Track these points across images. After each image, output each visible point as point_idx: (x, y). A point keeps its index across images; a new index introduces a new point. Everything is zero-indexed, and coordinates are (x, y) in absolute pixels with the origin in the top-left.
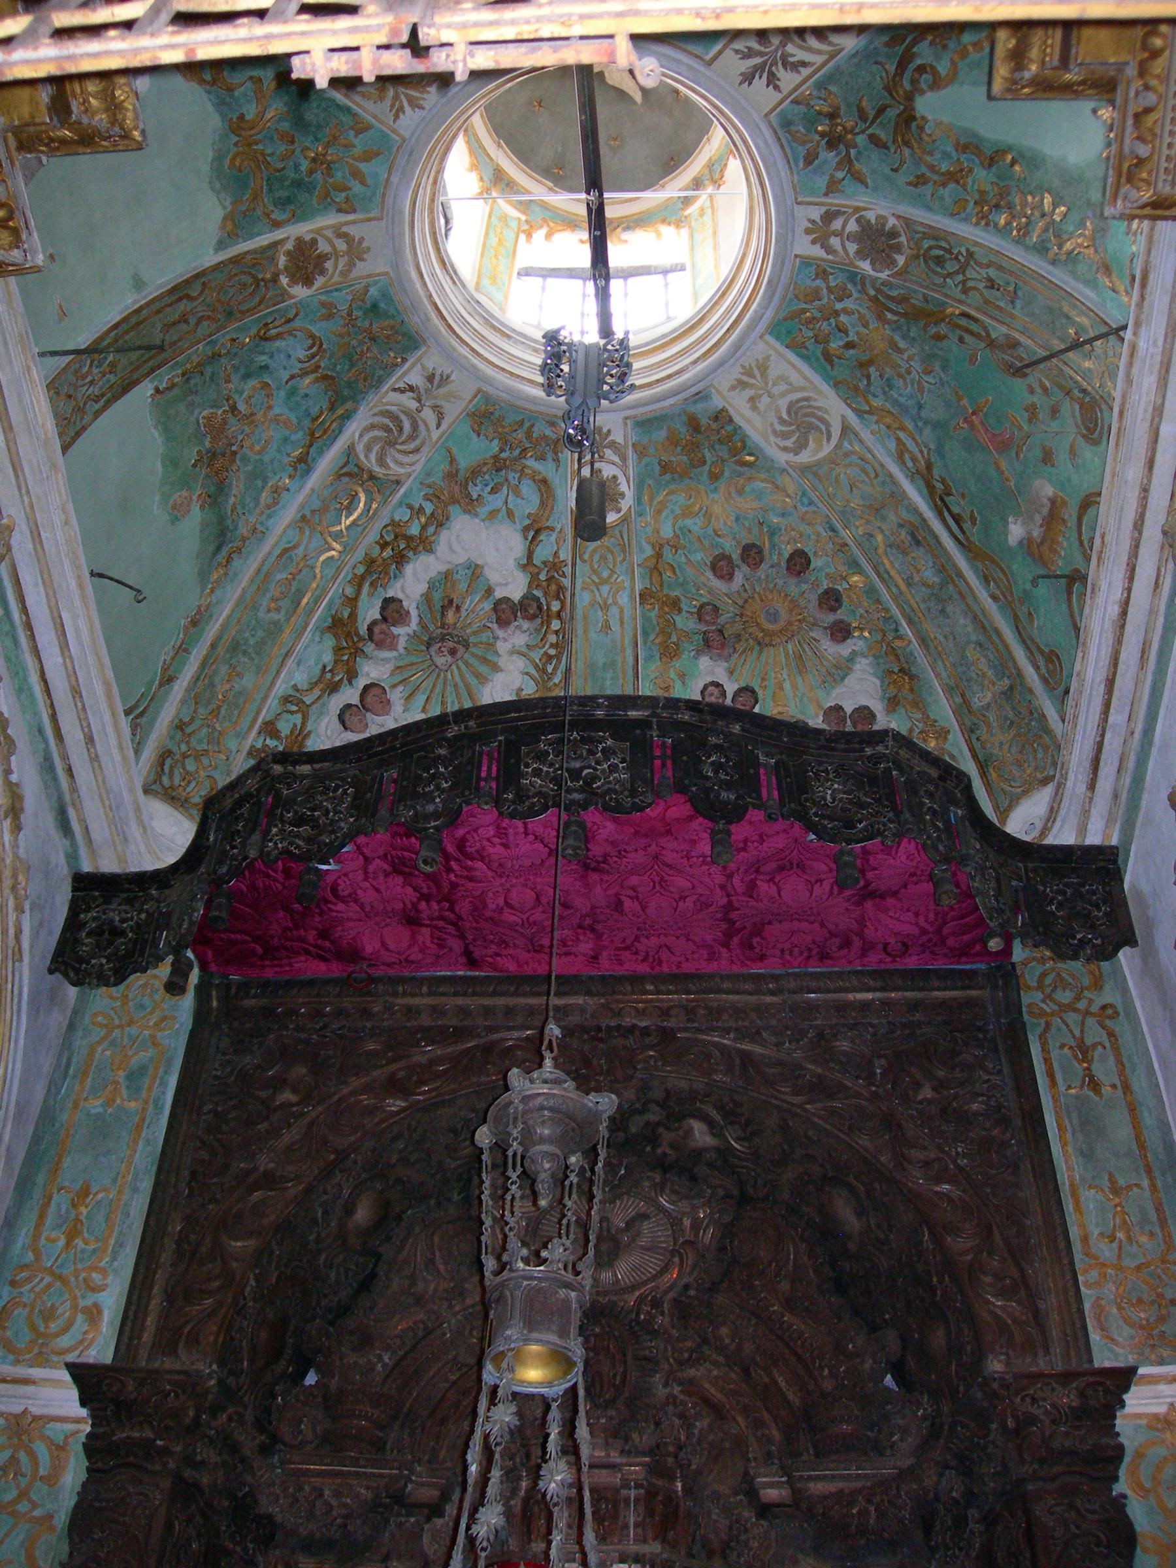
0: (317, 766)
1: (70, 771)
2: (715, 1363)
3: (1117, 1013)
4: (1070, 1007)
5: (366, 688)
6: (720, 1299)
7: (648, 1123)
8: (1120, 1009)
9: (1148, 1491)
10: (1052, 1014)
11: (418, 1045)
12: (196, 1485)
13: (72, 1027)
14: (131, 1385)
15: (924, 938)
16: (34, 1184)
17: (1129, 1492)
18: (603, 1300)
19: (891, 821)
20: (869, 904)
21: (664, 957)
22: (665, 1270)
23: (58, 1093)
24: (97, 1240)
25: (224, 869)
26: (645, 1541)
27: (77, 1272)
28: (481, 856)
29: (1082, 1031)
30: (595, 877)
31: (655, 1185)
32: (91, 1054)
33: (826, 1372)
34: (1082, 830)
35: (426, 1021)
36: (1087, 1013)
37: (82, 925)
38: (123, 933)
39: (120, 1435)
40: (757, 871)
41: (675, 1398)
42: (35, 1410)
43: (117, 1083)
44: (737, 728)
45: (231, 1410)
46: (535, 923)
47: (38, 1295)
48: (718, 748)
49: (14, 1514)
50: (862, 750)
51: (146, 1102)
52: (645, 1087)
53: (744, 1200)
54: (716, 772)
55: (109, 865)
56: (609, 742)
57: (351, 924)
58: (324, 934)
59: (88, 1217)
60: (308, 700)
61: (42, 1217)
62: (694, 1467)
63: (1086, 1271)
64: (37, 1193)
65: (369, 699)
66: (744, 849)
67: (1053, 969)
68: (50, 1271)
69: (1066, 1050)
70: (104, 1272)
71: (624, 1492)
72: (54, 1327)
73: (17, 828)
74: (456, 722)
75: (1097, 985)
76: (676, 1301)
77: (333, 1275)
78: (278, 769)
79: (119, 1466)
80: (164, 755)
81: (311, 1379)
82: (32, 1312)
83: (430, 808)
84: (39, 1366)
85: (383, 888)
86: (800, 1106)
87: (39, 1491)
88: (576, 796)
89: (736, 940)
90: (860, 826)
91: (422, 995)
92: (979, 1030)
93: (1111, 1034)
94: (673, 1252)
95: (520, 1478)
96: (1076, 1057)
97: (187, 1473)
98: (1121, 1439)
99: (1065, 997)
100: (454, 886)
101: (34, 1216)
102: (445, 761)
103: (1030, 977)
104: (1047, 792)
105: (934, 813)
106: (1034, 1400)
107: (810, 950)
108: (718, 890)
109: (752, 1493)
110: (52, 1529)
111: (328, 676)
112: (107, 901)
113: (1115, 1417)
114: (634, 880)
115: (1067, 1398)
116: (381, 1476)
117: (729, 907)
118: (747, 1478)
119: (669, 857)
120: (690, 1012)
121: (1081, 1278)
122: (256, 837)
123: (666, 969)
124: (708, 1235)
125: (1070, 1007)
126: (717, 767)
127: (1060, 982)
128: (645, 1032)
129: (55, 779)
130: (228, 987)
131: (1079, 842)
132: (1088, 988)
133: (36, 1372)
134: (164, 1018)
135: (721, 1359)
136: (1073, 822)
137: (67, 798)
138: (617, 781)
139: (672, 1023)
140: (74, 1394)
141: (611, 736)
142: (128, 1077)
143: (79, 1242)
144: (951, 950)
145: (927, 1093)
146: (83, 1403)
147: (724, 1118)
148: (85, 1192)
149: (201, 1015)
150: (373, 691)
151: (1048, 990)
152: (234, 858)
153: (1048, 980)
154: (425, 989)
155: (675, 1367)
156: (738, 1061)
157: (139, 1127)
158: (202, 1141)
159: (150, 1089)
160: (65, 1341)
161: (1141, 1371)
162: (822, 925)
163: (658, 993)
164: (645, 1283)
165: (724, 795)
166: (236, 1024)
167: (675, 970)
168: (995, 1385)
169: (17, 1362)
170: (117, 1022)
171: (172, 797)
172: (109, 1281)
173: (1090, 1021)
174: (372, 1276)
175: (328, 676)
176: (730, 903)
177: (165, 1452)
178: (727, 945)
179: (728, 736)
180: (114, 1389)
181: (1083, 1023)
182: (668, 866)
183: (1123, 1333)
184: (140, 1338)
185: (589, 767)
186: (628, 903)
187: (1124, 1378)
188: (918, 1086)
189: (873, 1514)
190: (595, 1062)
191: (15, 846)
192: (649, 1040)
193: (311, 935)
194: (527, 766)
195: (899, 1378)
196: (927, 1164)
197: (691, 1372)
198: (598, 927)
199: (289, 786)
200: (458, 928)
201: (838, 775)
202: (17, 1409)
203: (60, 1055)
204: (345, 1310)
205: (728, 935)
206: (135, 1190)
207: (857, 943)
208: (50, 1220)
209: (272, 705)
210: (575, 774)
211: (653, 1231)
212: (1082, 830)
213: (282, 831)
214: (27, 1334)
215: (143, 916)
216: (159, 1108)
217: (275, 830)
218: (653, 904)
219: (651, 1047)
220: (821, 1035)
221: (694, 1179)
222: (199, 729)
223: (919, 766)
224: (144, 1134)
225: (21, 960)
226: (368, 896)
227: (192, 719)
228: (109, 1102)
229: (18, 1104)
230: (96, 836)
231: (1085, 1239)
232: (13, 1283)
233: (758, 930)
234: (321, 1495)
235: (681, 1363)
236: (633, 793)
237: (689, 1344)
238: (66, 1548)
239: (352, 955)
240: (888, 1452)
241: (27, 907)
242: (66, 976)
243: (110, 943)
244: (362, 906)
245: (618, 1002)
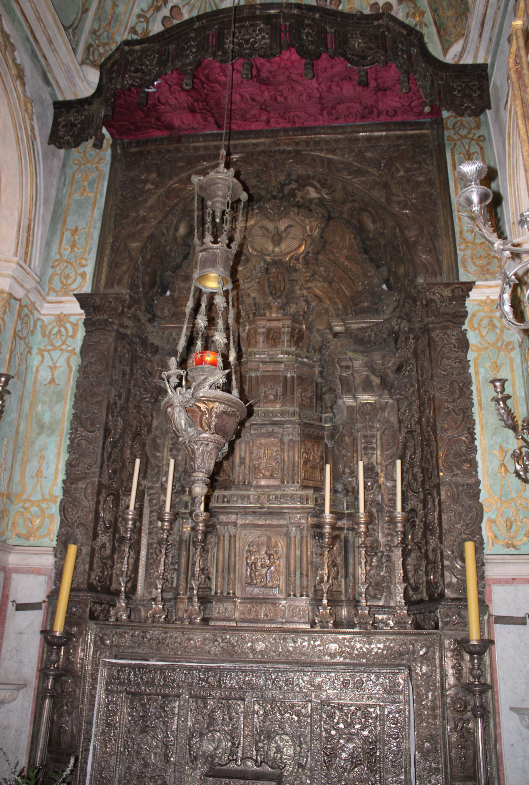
0: (143, 46)
1: (44, 57)
2: (319, 281)
3: (485, 139)
4: (465, 137)
5: (172, 8)
6: (321, 257)
7: (291, 189)
8: (487, 137)
9: (476, 329)
10: (458, 140)
11: (199, 162)
12: (126, 334)
13: (64, 166)
14: (98, 300)
15: (403, 109)
16: (57, 229)
17: (468, 329)
18: (277, 259)
19: (382, 56)
20: (379, 94)
21: (296, 120)
22: (300, 246)
23: (62, 192)
24: (82, 248)
25: (108, 95)
26: (290, 347)
27: (76, 261)
28: (216, 81)
29: (469, 147)
30: (264, 87)
31: (295, 213)
32: (73, 176)
33: (360, 284)
34: (476, 57)
35: (202, 152)
36: (472, 139)
37: (59, 124)
38: (75, 125)
39: (96, 318)
40: (331, 81)
41: (303, 294)
42: (65, 312)
43: (84, 186)
44: (317, 16)
45: (136, 306)
46: (242, 109)
47: (63, 270)
48: (309, 26)
49: (61, 350)
50: (373, 23)
51: (96, 193)
52: (289, 175)
53: (330, 218)
54: (307, 37)
55: (70, 97)
56: (262, 26)
57: (168, 114)
58: (158, 119)
59: (78, 239)
60: (148, 16)
61: (61, 241)
62: (310, 320)
63: (460, 245)
64: (59, 232)
65: (174, 13)
66: (325, 72)
67: (460, 121)
68: (66, 261)
69: (462, 155)
70: (86, 260)
71: (283, 329)
72: (69, 281)
73: (23, 84)
74: (198, 21)
75: (478, 127)
76: (304, 258)
77: (173, 255)
78: (127, 48)
79: (95, 330)
80: (89, 47)
81: (168, 293)
82: (61, 277)
83: (188, 61)
84: (65, 296)
85: (178, 97)
86: (350, 180)
87: (69, 341)
88: (247, 51)
89: (325, 112)
90: (369, 58)
91: (200, 142)
92: (425, 147)
93: (481, 148)
94: (304, 239)
95: (246, 325)
96: (465, 158)
97: (121, 330)
98: (467, 309)
99: (463, 132)
100: (207, 95)
101: (58, 241)
102: (194, 39)
103: (450, 123)
104: (463, 39)
105: (403, 51)
106: (434, 294)
107: (356, 115)
108: (315, 90)
109: (331, 329)
110: (75, 354)
111: (156, 3)
112: (68, 112)
113: (465, 300)
114: (281, 87)
115: (447, 293)
117: (321, 98)
118: (329, 324)
119: (294, 77)
120: (307, 143)
121: (458, 247)
122: (120, 79)
123: (297, 125)
124: (316, 233)
125: (465, 137)
126: (308, 34)
127: (462, 126)
128: (289, 152)
129: (39, 61)
130: (123, 144)
131: (474, 62)
132: (474, 129)
133: (63, 299)
134: (101, 159)
135: (321, 280)
136: (472, 53)
137: (46, 69)
138: (265, 43)
139: (300, 148)
140: (78, 304)
141: (263, 23)
142: (89, 184)
143: (76, 249)
144: (415, 113)
145: (402, 173)
146: (82, 308)
147: (321, 186)
148: (76, 229)
149: (114, 157)
150: (175, 9)
151: (457, 130)
152: (112, 89)
153: (458, 125)
154: (201, 139)
156: (326, 163)
157: (95, 203)
158: (118, 207)
159: (97, 188)
160: (74, 286)
161: (477, 283)
162: (360, 103)
163: (295, 135)
164: (292, 252)
165: (310, 47)
166: (128, 159)
167: (301, 126)
168: (419, 288)
169: (57, 295)
170: (82, 162)
171: (93, 64)
172: (88, 263)
173: (474, 143)
174: (188, 254)
175: (156, 3)
176: (321, 96)
177: (112, 323)
178: (321, 114)
179: (313, 19)
180: (92, 302)
181: (470, 143)
182: (293, 80)
183: (472, 268)
184: (100, 282)
185: (253, 38)
186: (279, 98)
187: (469, 286)
188: (398, 170)
189: (373, 336)
190: (269, 165)
191: (24, 91)
192: (290, 156)
193: (153, 120)
194: (227, 39)
195: (388, 286)
196: (400, 202)
197: (310, 285)
198: (268, 109)
199: (132, 55)
200: (211, 113)
201: (361, 36)
202: (58, 312)
203: (60, 178)
204: (179, 267)
205: (322, 110)
206: (95, 227)
207: (375, 111)
208: (64, 242)
209: (133, 20)
210: (247, 41)
211: (295, 231)
212: (476, 57)
213: (130, 76)
214: (60, 285)
215: (83, 117)
216: (101, 195)
217: (127, 76)
218: (289, 98)
219: (291, 158)
220: (360, 151)
221: (310, 210)
222: (103, 33)
223: (398, 29)
224: (97, 205)
225: (35, 139)
226: (173, 102)
227: (99, 29)
228: (82, 194)
229: (44, 198)
230: (61, 85)
231: (461, 232)
232: (53, 267)
233: (334, 108)
234: (172, 335)
235: (306, 281)
236: (271, 48)
237: (309, 274)
238: (80, 360)
239: (170, 127)
240: (381, 314)
241: (35, 118)
242: (55, 145)
243: (71, 130)
244: (171, 106)
245: (278, 140)
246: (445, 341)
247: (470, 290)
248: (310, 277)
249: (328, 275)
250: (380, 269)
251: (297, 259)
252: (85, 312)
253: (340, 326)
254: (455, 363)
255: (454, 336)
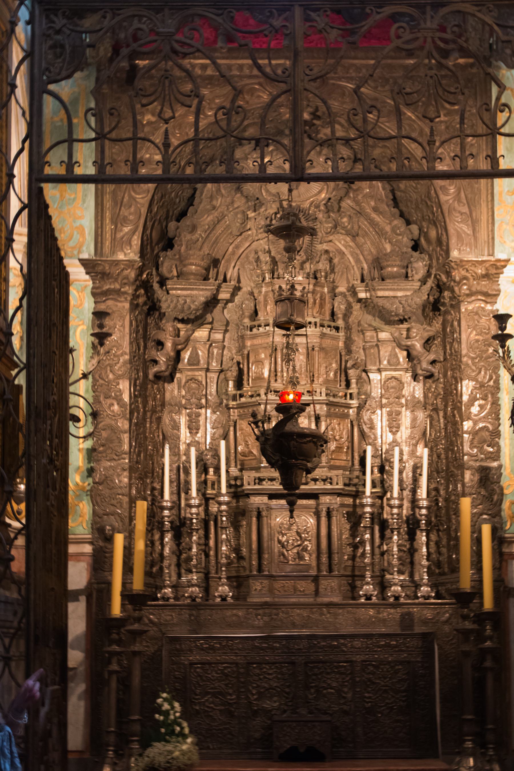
116: (206, 289)
146: (87, 273)
155: (324, 235)
235: (327, 233)
246: (476, 322)
247: (505, 266)
248: (332, 228)
249: (353, 228)
250: (410, 226)
251: (317, 207)
252: (93, 280)
253: (366, 291)
254: (485, 346)
255: (485, 316)
